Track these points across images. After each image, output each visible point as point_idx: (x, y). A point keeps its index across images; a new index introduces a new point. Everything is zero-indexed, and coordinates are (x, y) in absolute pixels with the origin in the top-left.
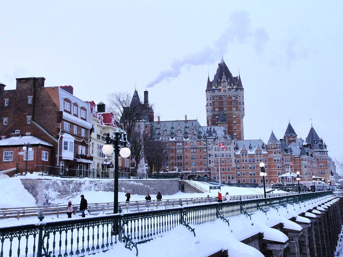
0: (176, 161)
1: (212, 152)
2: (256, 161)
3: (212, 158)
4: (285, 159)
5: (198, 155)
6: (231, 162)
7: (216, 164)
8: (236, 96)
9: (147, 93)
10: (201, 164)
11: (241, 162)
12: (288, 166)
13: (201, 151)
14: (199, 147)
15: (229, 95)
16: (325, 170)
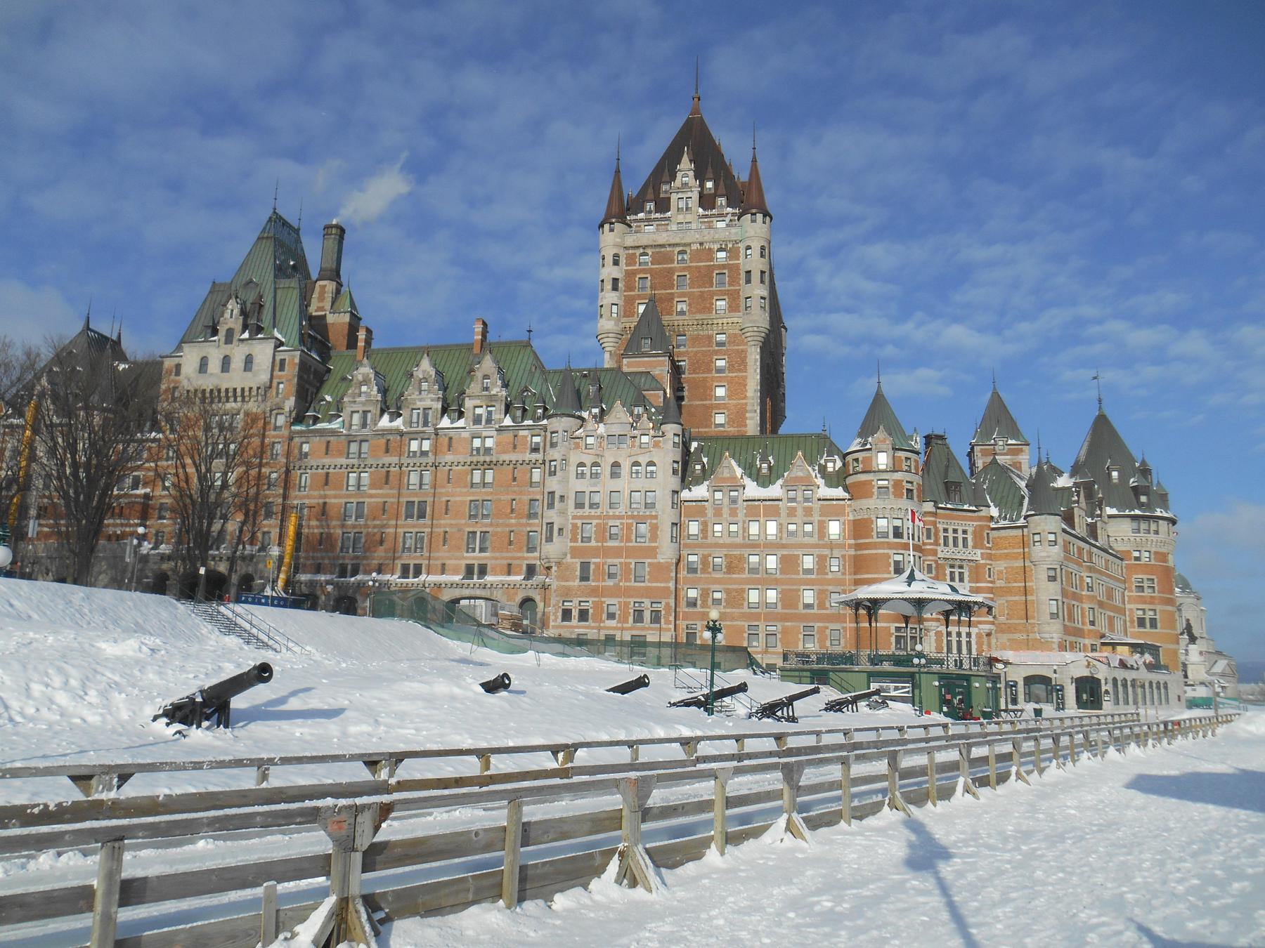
0: (396, 526)
1: (565, 481)
2: (785, 535)
3: (563, 513)
4: (946, 530)
5: (502, 498)
6: (654, 537)
7: (579, 544)
8: (730, 246)
9: (334, 231)
10: (510, 543)
11: (706, 537)
12: (957, 571)
13: (515, 479)
14: (506, 457)
15: (701, 244)
16: (1159, 608)
